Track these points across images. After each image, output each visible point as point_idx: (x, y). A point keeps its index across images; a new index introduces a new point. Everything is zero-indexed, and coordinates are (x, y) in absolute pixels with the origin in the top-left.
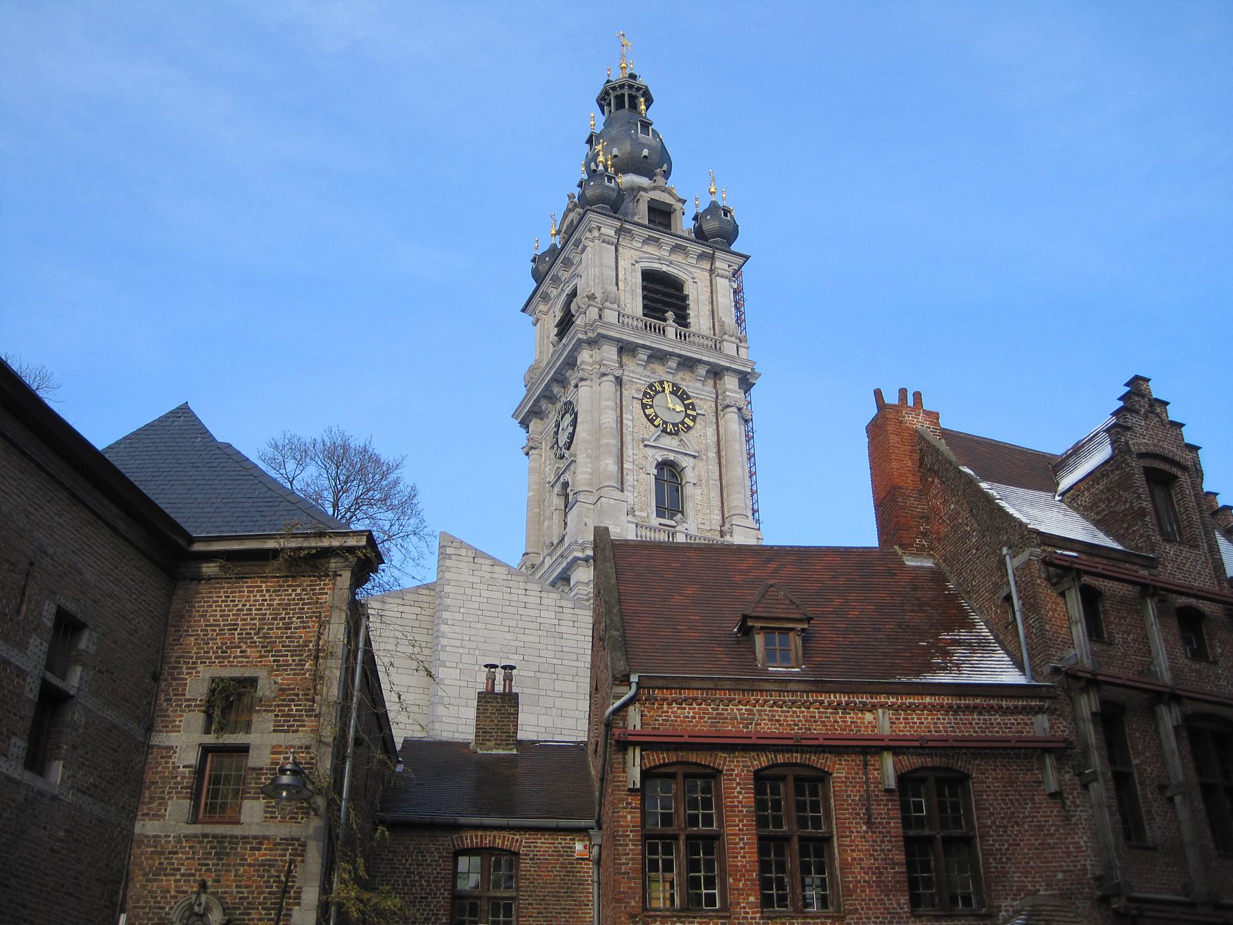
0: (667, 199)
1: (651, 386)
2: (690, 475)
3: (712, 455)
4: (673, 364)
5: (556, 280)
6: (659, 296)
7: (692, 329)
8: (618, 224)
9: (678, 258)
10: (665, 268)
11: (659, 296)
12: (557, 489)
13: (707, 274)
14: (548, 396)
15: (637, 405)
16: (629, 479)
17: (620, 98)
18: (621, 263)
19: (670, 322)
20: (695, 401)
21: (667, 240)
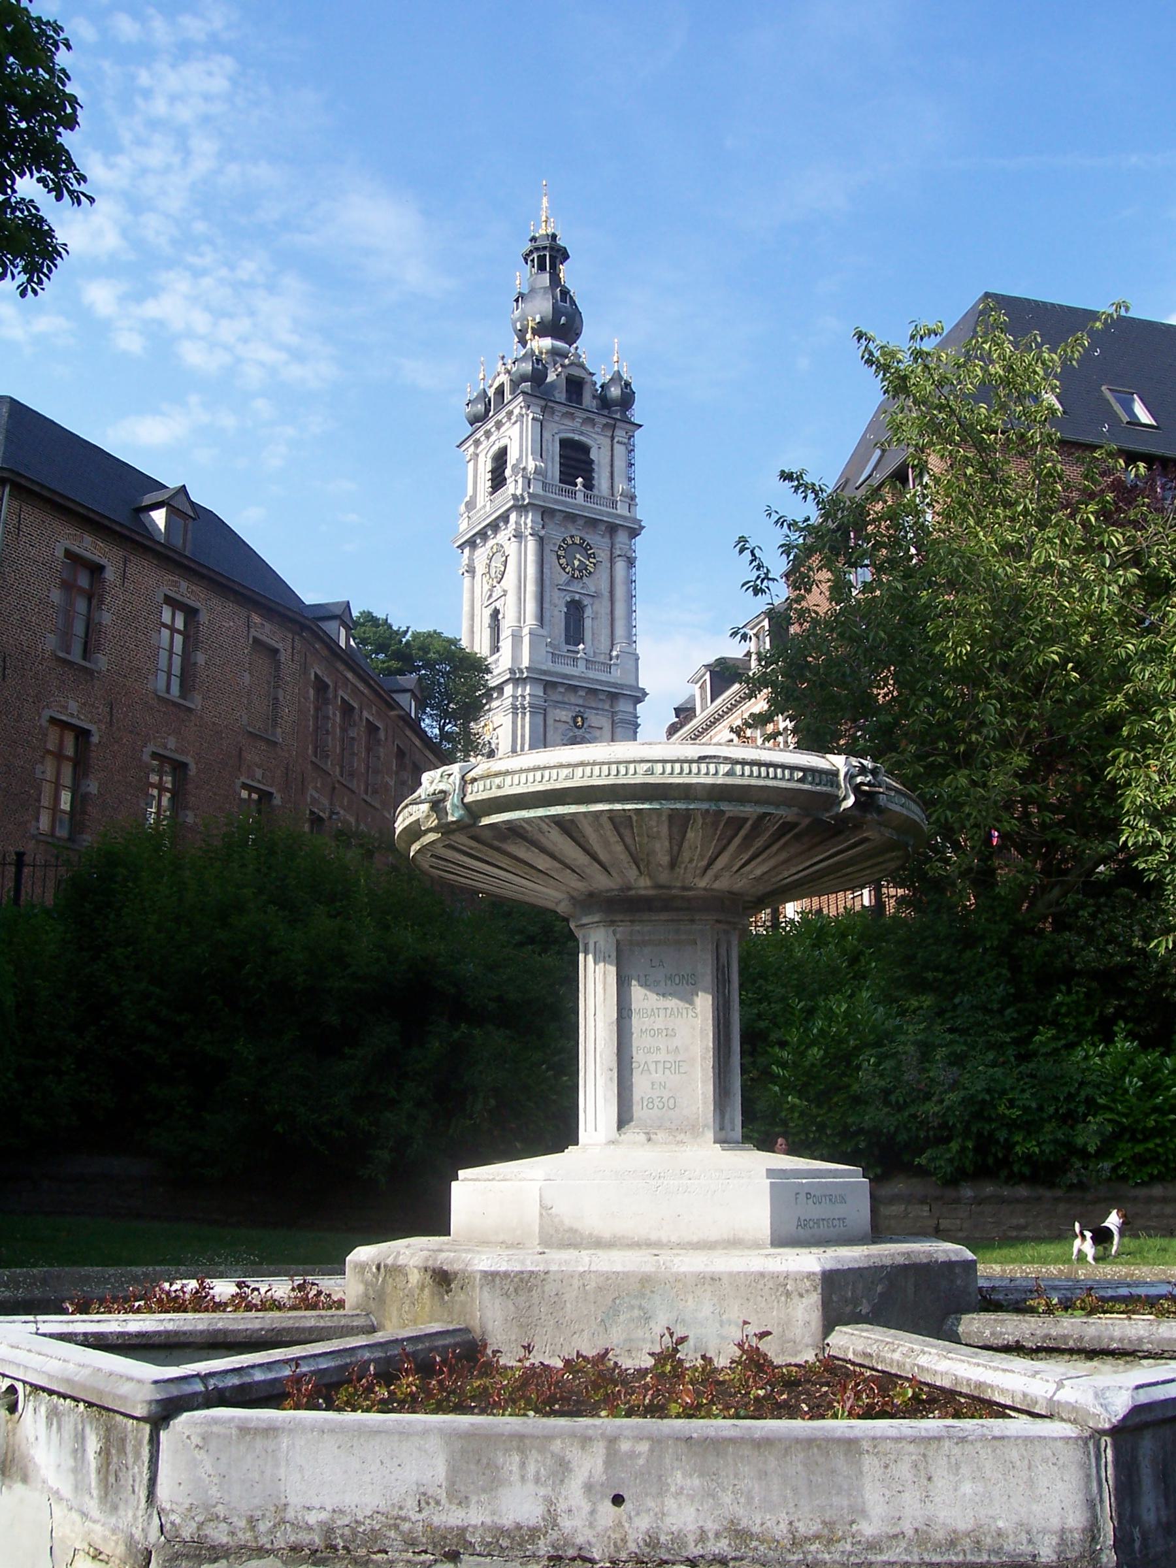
0: (583, 374)
1: (564, 540)
2: (588, 612)
3: (606, 594)
4: (581, 522)
5: (488, 434)
6: (573, 463)
7: (596, 492)
8: (543, 403)
9: (587, 428)
10: (577, 437)
11: (573, 463)
12: (488, 612)
13: (608, 441)
14: (483, 534)
15: (555, 557)
16: (547, 615)
17: (542, 259)
18: (545, 434)
19: (579, 486)
20: (597, 552)
21: (581, 415)
